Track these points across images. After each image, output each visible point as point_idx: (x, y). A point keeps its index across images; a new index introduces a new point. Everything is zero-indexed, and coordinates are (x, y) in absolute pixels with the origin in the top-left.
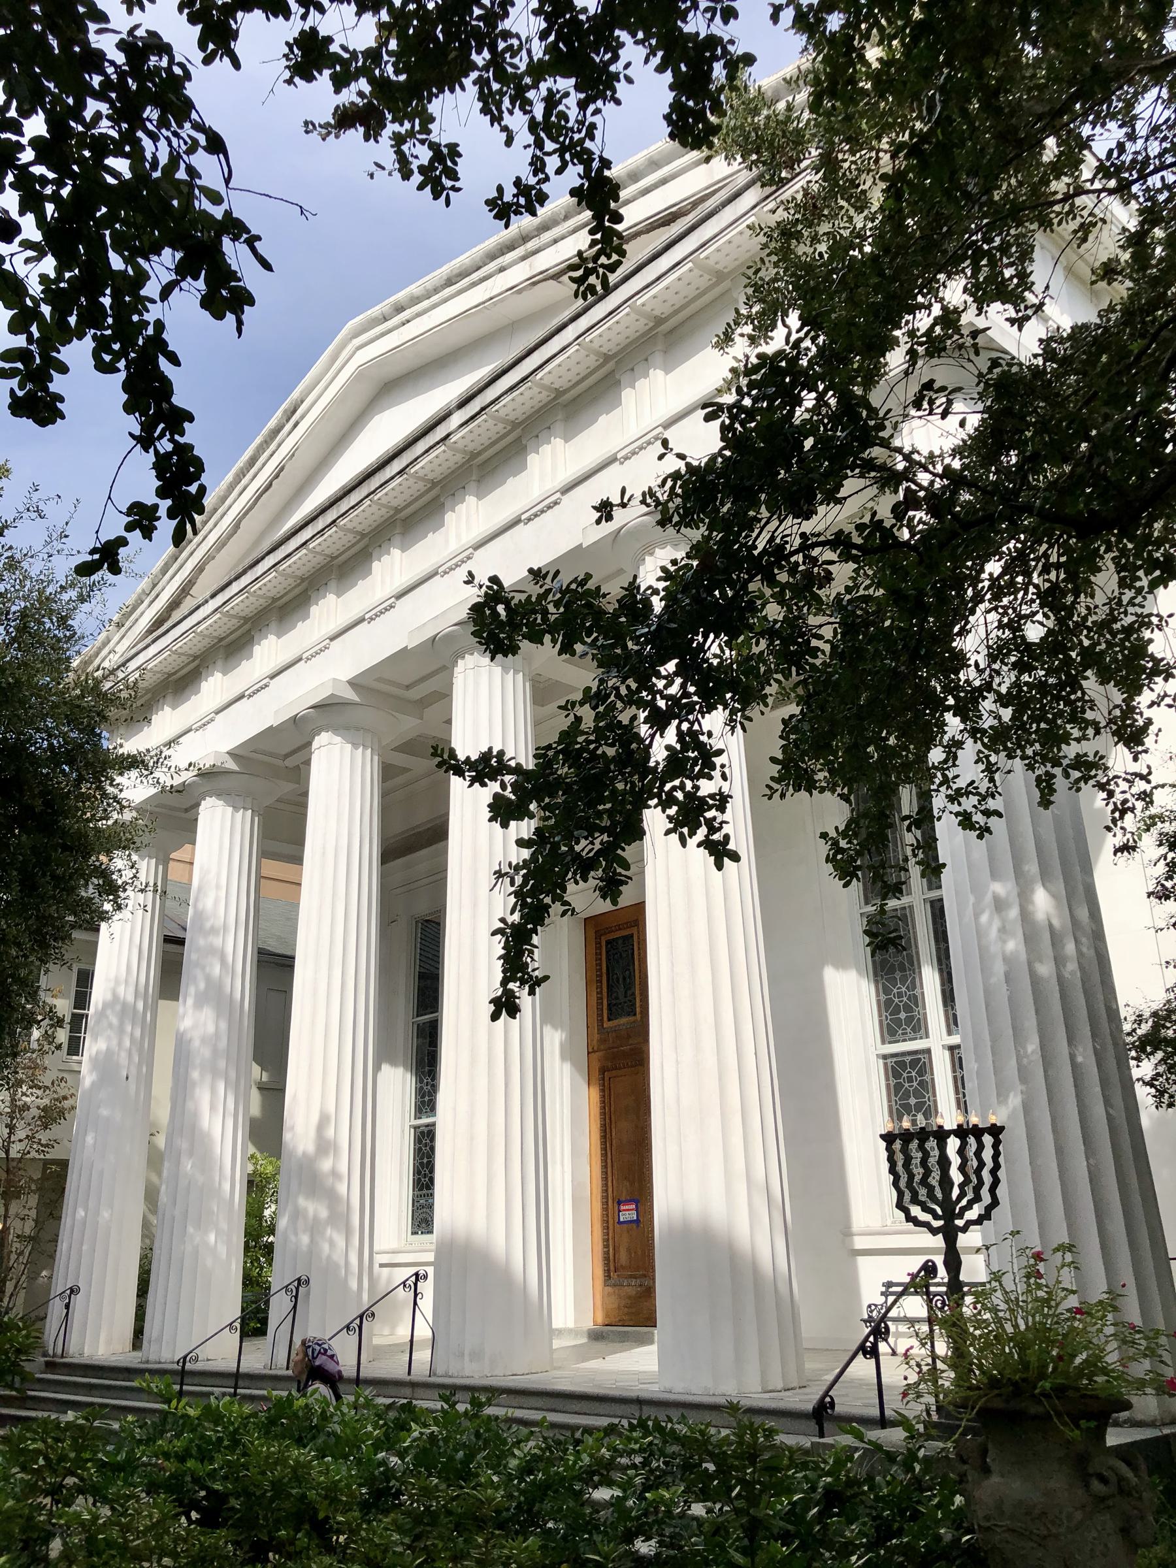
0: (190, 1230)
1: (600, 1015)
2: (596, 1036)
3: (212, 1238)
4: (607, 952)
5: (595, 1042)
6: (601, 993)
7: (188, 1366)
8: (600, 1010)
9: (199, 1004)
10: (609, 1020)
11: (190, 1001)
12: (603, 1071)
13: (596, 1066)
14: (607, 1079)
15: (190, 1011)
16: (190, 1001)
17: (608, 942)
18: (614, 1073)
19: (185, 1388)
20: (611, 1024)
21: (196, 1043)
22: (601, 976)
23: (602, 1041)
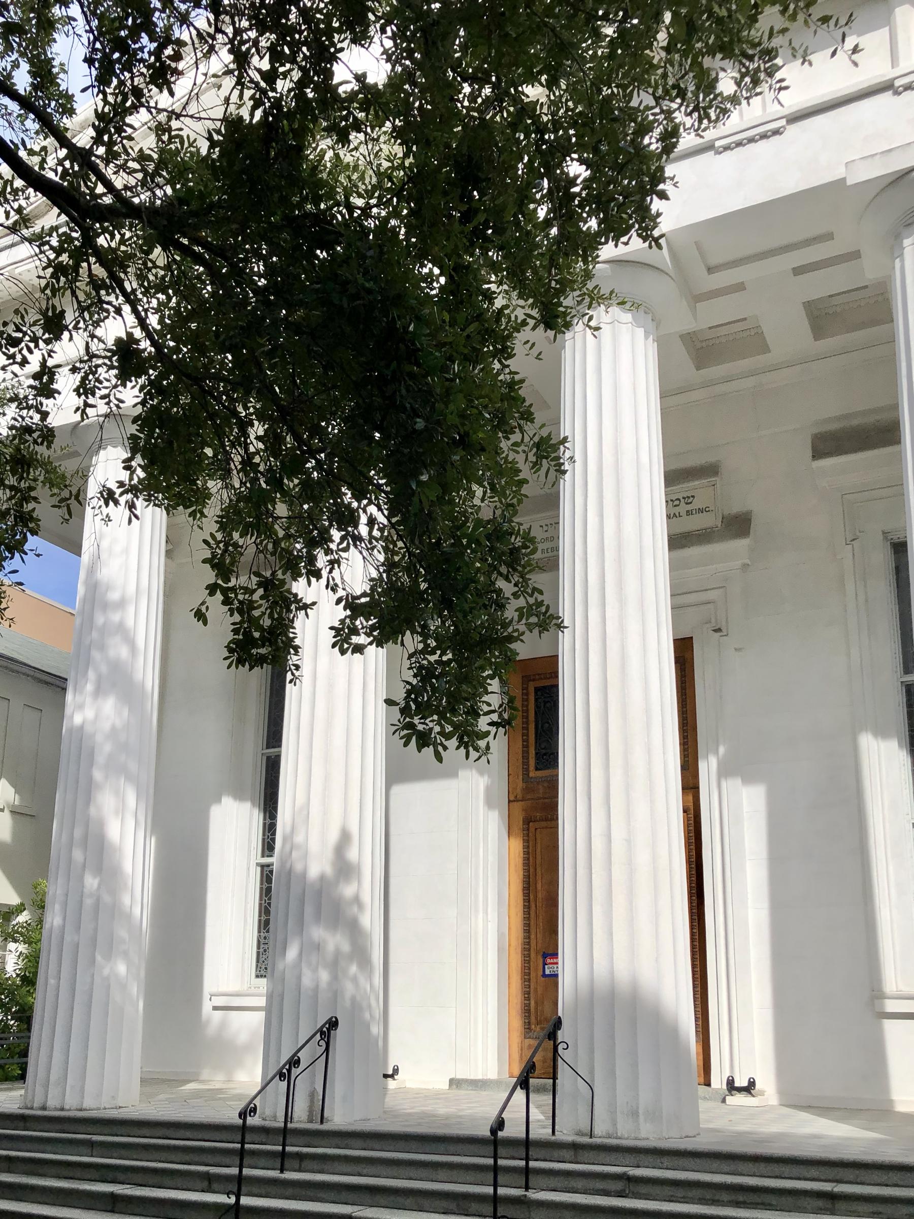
0: (99, 958)
1: (526, 763)
2: (520, 784)
3: (122, 968)
4: (536, 700)
5: (519, 791)
6: (527, 741)
7: (250, 1121)
8: (525, 756)
9: (98, 692)
10: (537, 769)
11: (90, 687)
12: (527, 821)
13: (519, 817)
14: (532, 830)
15: (89, 700)
16: (90, 687)
17: (537, 690)
18: (544, 824)
19: (288, 1149)
20: (539, 774)
21: (99, 738)
22: (527, 723)
23: (527, 790)
